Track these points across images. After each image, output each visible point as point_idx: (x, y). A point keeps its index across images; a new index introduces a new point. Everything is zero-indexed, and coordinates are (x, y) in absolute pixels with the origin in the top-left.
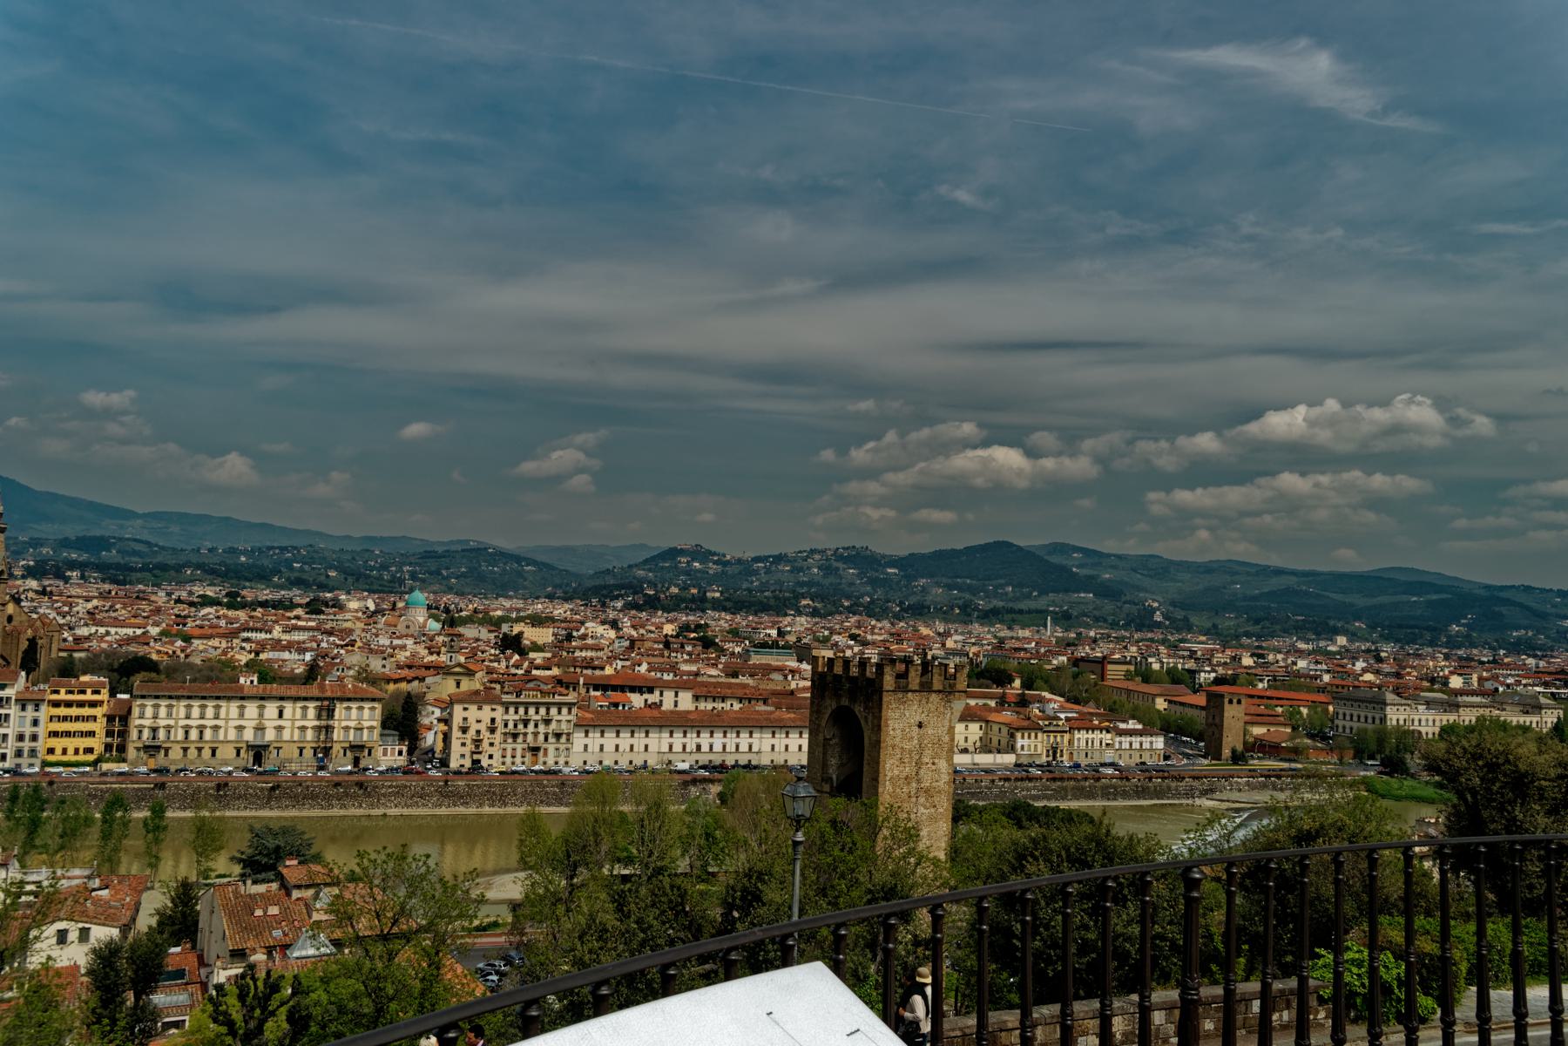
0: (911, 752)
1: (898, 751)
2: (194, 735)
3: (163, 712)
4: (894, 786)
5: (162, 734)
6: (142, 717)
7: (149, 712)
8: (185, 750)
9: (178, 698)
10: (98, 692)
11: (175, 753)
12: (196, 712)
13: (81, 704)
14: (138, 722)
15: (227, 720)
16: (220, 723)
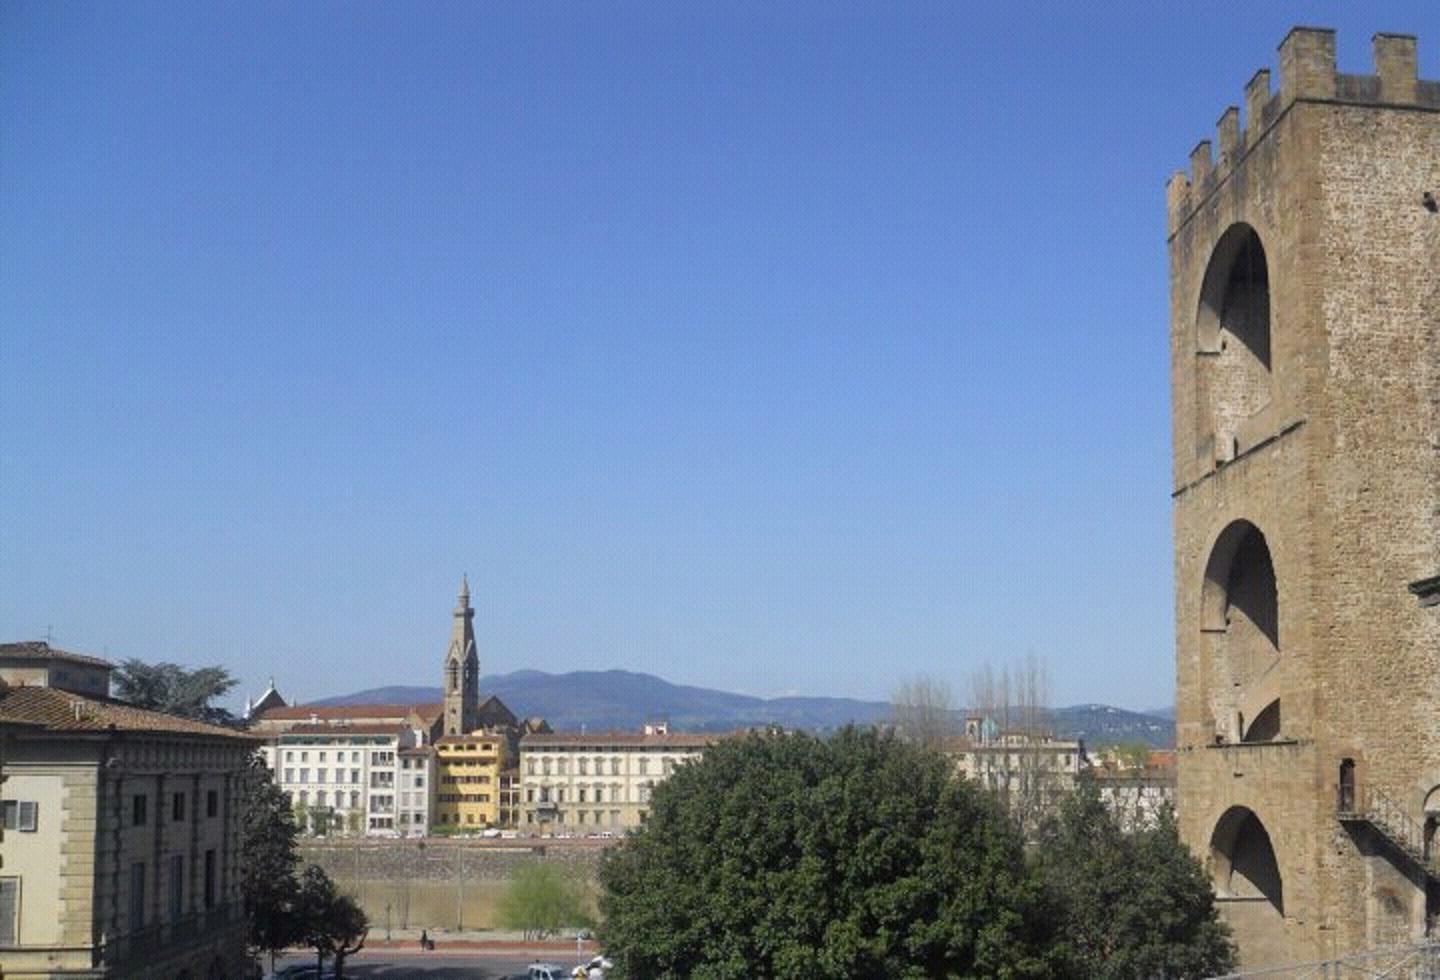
0: (1403, 274)
1: (1361, 269)
2: (590, 796)
3: (554, 767)
4: (1355, 363)
5: (554, 795)
6: (532, 773)
7: (539, 767)
8: (582, 815)
9: (573, 749)
10: (487, 747)
11: (572, 818)
12: (591, 767)
13: (471, 762)
14: (528, 780)
15: (628, 776)
16: (620, 780)
